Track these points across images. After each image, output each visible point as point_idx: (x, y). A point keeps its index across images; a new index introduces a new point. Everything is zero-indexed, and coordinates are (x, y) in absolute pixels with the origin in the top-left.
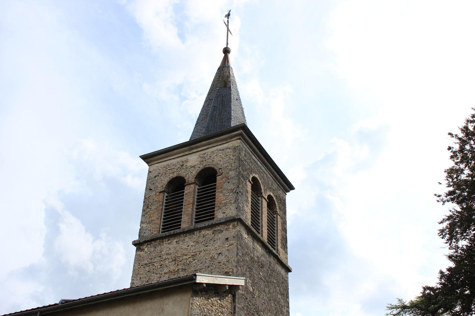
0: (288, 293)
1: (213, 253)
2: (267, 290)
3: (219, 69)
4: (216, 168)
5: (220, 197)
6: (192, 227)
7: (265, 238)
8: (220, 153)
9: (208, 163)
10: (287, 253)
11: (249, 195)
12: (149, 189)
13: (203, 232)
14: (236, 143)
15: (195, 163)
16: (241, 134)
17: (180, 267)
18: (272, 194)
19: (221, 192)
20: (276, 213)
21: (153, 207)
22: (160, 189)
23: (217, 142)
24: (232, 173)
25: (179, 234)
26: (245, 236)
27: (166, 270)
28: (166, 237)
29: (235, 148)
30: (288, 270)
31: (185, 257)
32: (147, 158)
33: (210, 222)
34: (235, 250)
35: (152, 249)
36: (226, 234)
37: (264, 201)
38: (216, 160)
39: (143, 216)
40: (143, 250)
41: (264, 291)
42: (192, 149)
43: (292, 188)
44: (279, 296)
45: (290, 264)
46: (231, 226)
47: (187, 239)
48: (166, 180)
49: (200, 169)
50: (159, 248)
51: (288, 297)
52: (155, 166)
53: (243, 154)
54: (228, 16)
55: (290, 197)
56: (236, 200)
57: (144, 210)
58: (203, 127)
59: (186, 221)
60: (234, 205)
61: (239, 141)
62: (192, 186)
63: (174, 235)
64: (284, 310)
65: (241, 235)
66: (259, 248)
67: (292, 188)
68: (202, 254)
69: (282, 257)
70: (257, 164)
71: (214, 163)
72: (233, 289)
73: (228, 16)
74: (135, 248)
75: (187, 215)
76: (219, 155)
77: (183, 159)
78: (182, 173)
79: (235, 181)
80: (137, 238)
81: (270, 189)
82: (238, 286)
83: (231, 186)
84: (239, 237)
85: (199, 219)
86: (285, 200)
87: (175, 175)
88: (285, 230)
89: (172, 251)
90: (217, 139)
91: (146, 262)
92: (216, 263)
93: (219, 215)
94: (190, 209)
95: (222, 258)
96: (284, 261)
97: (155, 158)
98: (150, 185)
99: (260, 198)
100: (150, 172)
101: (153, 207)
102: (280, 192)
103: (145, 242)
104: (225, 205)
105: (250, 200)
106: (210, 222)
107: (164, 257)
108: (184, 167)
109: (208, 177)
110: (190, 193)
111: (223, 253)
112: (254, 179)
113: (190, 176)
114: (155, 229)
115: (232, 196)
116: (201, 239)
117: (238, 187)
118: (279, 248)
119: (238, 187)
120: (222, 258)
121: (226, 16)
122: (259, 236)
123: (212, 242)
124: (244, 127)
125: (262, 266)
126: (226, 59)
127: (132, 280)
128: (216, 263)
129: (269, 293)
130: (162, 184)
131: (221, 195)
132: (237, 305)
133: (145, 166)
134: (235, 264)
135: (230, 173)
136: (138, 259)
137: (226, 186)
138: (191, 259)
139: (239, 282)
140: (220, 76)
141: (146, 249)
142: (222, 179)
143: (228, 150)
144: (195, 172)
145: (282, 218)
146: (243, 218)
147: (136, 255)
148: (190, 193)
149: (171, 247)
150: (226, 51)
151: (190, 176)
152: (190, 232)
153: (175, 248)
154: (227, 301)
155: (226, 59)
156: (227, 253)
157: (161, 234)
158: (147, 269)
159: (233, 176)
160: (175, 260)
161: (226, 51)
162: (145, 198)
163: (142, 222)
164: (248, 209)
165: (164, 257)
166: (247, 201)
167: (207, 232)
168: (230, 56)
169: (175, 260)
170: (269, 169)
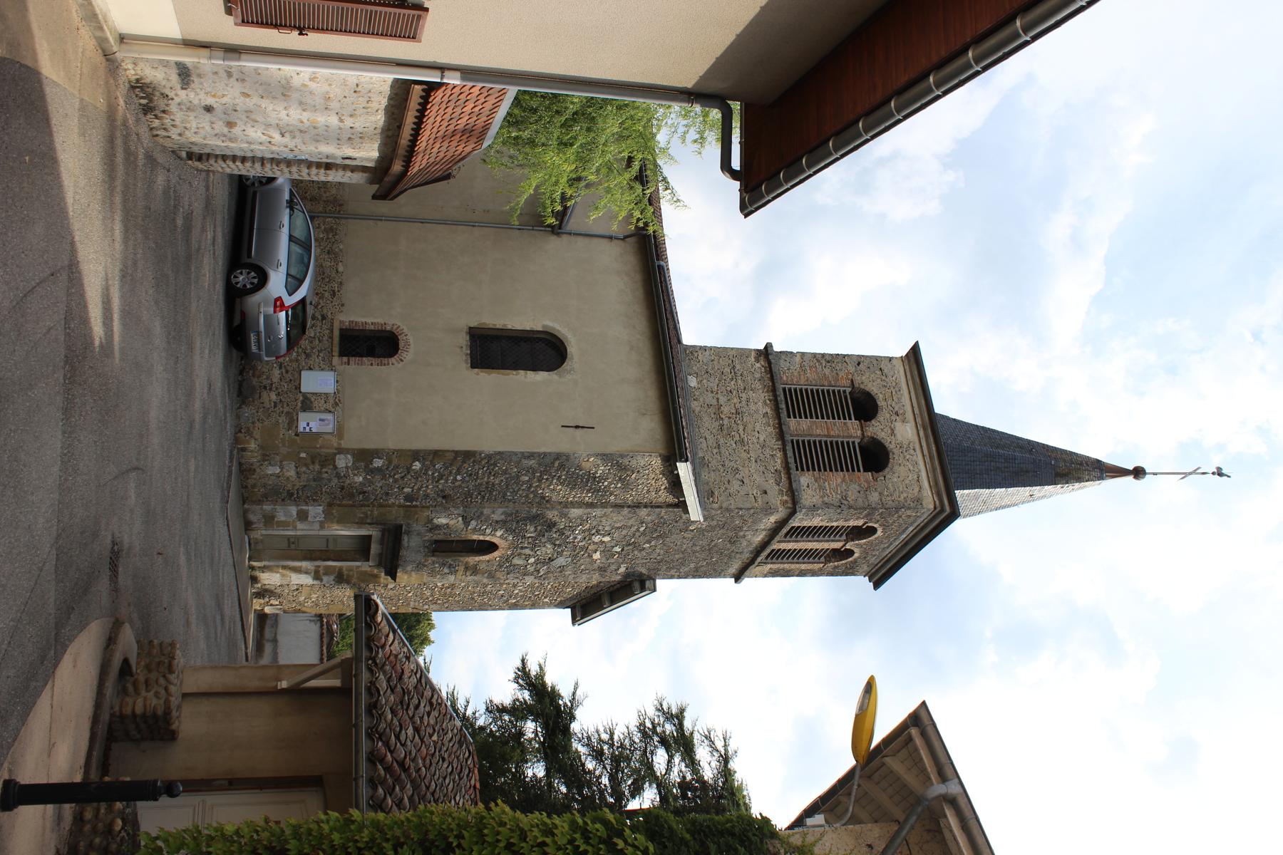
0: (700, 577)
1: (744, 472)
2: (698, 548)
3: (1099, 461)
4: (887, 470)
5: (836, 480)
6: (788, 438)
7: (775, 546)
8: (913, 477)
9: (896, 457)
10: (765, 576)
11: (841, 523)
12: (859, 360)
13: (779, 454)
14: (929, 501)
15: (899, 436)
16: (942, 510)
17: (726, 421)
18: (856, 555)
19: (844, 480)
20: (828, 560)
21: (827, 371)
22: (858, 379)
23: (934, 470)
24: (874, 497)
25: (778, 417)
26: (773, 519)
27: (722, 400)
28: (775, 396)
29: (918, 500)
30: (738, 578)
31: (741, 428)
32: (915, 350)
33: (793, 466)
34: (749, 506)
35: (758, 375)
36: (773, 489)
37: (840, 544)
38: (901, 471)
39: (814, 355)
40: (757, 360)
41: (694, 545)
42: (925, 429)
43: (877, 585)
44: (692, 565)
45: (747, 582)
46: (785, 498)
47: (770, 429)
48: (874, 388)
49: (887, 445)
50: (758, 385)
51: (694, 577)
52: (900, 368)
53: (909, 513)
54: (1220, 473)
55: (861, 583)
56: (827, 505)
57: (823, 355)
58: (973, 443)
59: (799, 426)
60: (820, 501)
61: (932, 507)
62: (859, 433)
63: (777, 409)
64: (672, 572)
65: (772, 514)
66: (759, 538)
67: (877, 585)
68: (744, 455)
69: (753, 569)
70: (901, 534)
71: (896, 467)
72: (683, 505)
73: (1220, 473)
74: (762, 347)
75: (810, 428)
76: (911, 473)
77: (910, 415)
78: (883, 415)
79: (860, 503)
80: (777, 348)
81: (865, 553)
82: (687, 512)
83: (852, 496)
84: (768, 510)
85: (797, 445)
86: (853, 574)
87: (881, 403)
88: (802, 574)
89: (753, 407)
90: (939, 470)
91: (738, 367)
92: (729, 477)
93: (805, 479)
94: (818, 432)
95: (736, 485)
96: (747, 573)
97: (914, 367)
98: (867, 362)
99: (844, 537)
100: (890, 359)
101: (827, 371)
102: (866, 568)
103: (770, 363)
104: (821, 488)
105: (835, 524)
106: (793, 466)
107: (744, 395)
108: (893, 418)
109: (875, 457)
110: (849, 430)
111: (744, 487)
112: (874, 530)
113: (877, 429)
114: (789, 376)
115: (834, 498)
116: (768, 452)
117: (850, 507)
118: (769, 566)
119: (850, 507)
120: (736, 485)
121: (1219, 469)
122: (777, 538)
123: (762, 469)
124: (954, 515)
125: (732, 543)
126: (1119, 472)
127: (711, 348)
128: (729, 477)
129: (694, 552)
130: (866, 382)
131: (839, 480)
132: (663, 511)
133: (901, 350)
134: (724, 505)
135: (876, 494)
136: (743, 353)
137: (854, 487)
138: (737, 438)
139: (695, 513)
140: (1081, 464)
141: (758, 365)
142: (867, 481)
143: (917, 489)
144: (883, 436)
145: (821, 569)
146: (799, 516)
147: (750, 350)
148: (849, 430)
149: (759, 404)
150: (1138, 473)
151: (877, 429)
152: (781, 435)
153: (757, 411)
154: (665, 497)
155: (1119, 472)
156: (742, 493)
157: (780, 387)
158: (727, 370)
159: (870, 498)
160: (737, 413)
161: (1138, 473)
162: (844, 356)
163: (803, 354)
164: (817, 522)
165: (744, 395)
166: (830, 520)
167: (779, 461)
168: (1130, 479)
169: (737, 413)
170: (898, 551)
